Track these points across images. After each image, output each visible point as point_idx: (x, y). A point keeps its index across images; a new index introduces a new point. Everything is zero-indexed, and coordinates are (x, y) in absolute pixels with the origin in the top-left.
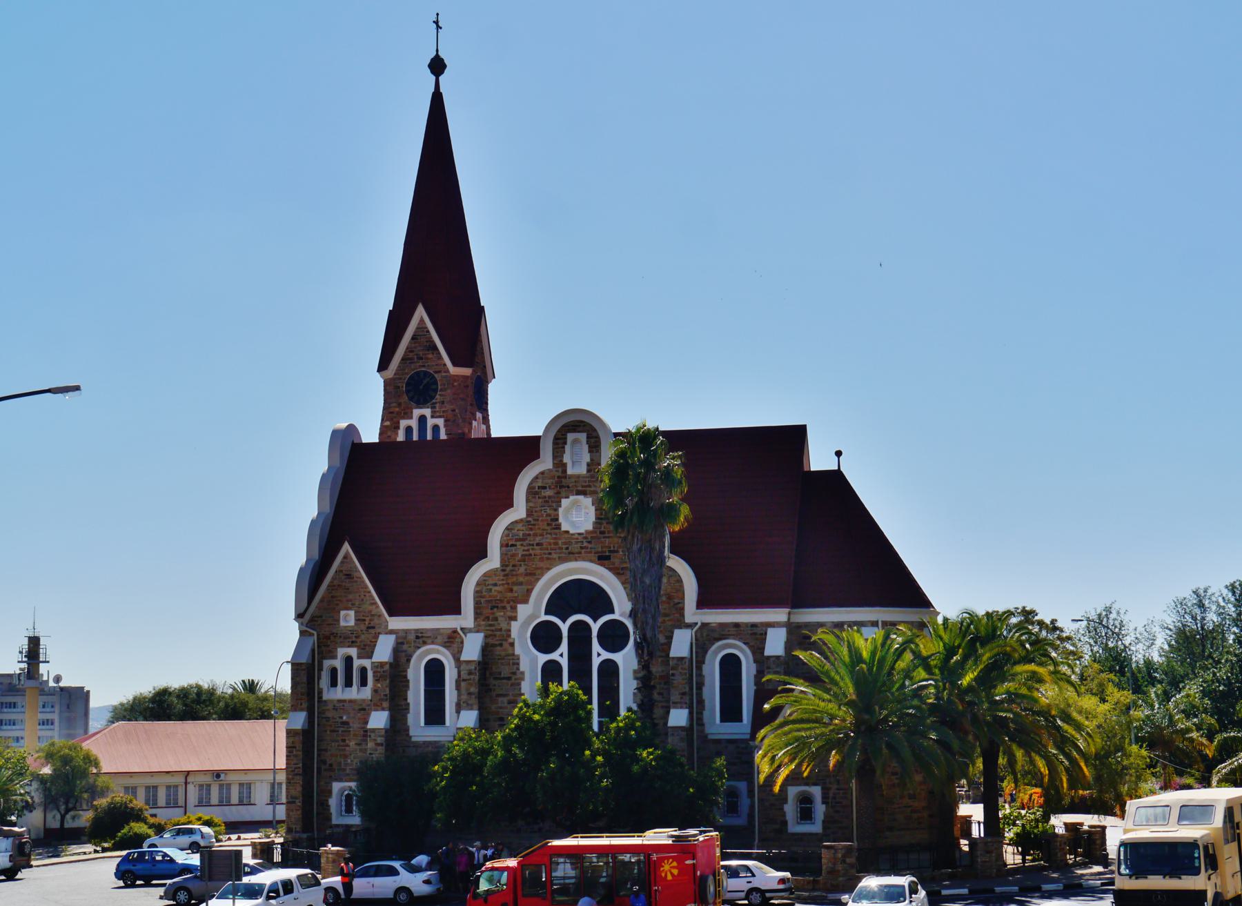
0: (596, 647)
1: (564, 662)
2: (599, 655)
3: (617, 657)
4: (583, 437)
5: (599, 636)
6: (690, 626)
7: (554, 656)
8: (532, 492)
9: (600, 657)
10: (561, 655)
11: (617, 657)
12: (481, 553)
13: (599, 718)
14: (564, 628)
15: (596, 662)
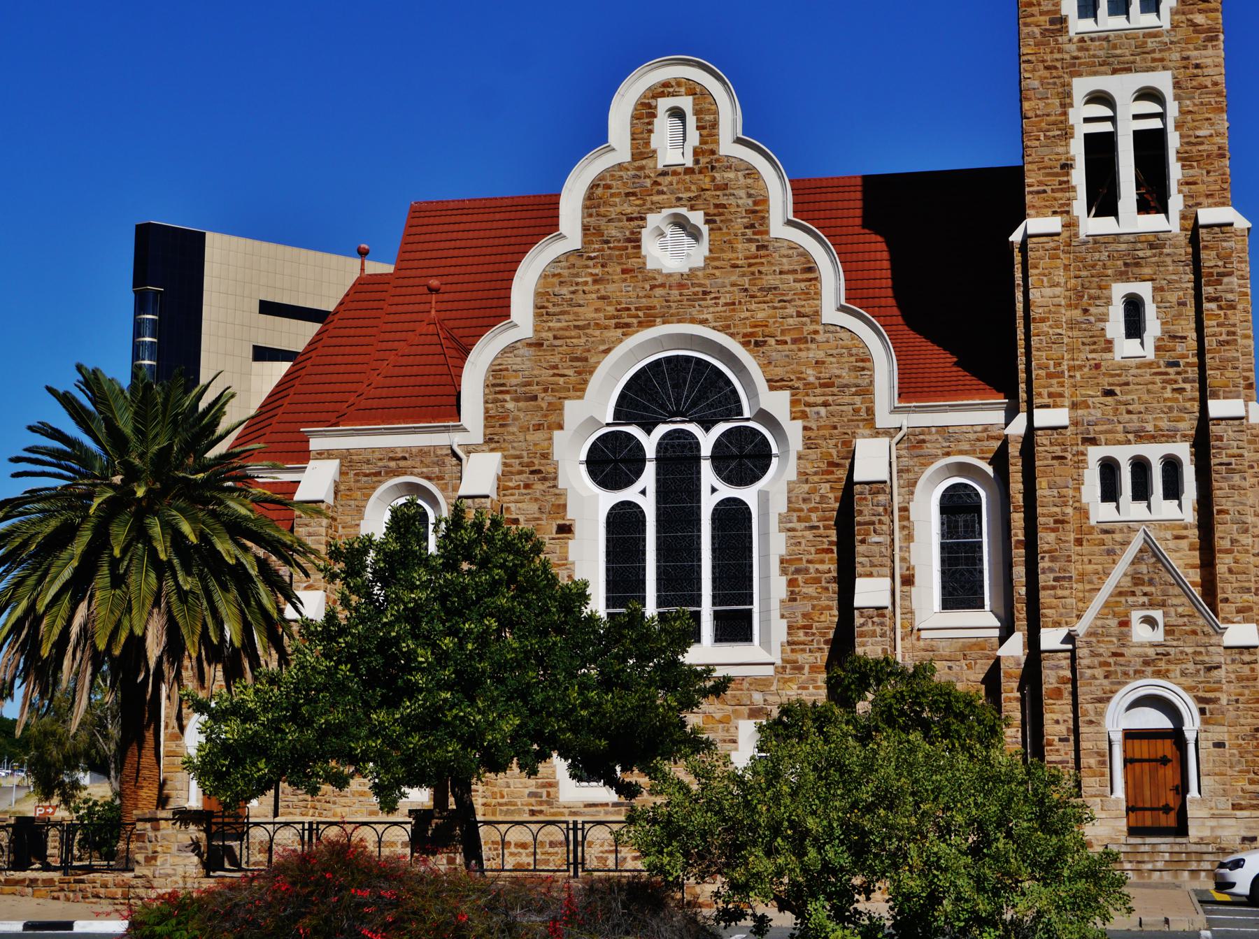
0: (708, 474)
1: (649, 506)
2: (714, 490)
3: (748, 495)
4: (686, 103)
5: (714, 458)
6: (887, 432)
7: (629, 494)
8: (594, 200)
9: (715, 494)
10: (643, 492)
11: (748, 495)
12: (500, 312)
13: (714, 604)
14: (650, 443)
15: (708, 504)
